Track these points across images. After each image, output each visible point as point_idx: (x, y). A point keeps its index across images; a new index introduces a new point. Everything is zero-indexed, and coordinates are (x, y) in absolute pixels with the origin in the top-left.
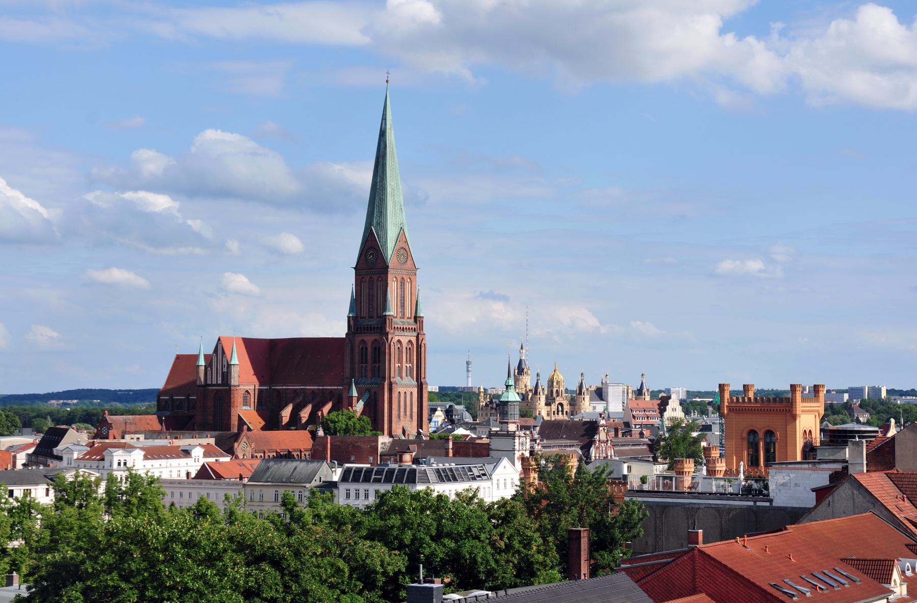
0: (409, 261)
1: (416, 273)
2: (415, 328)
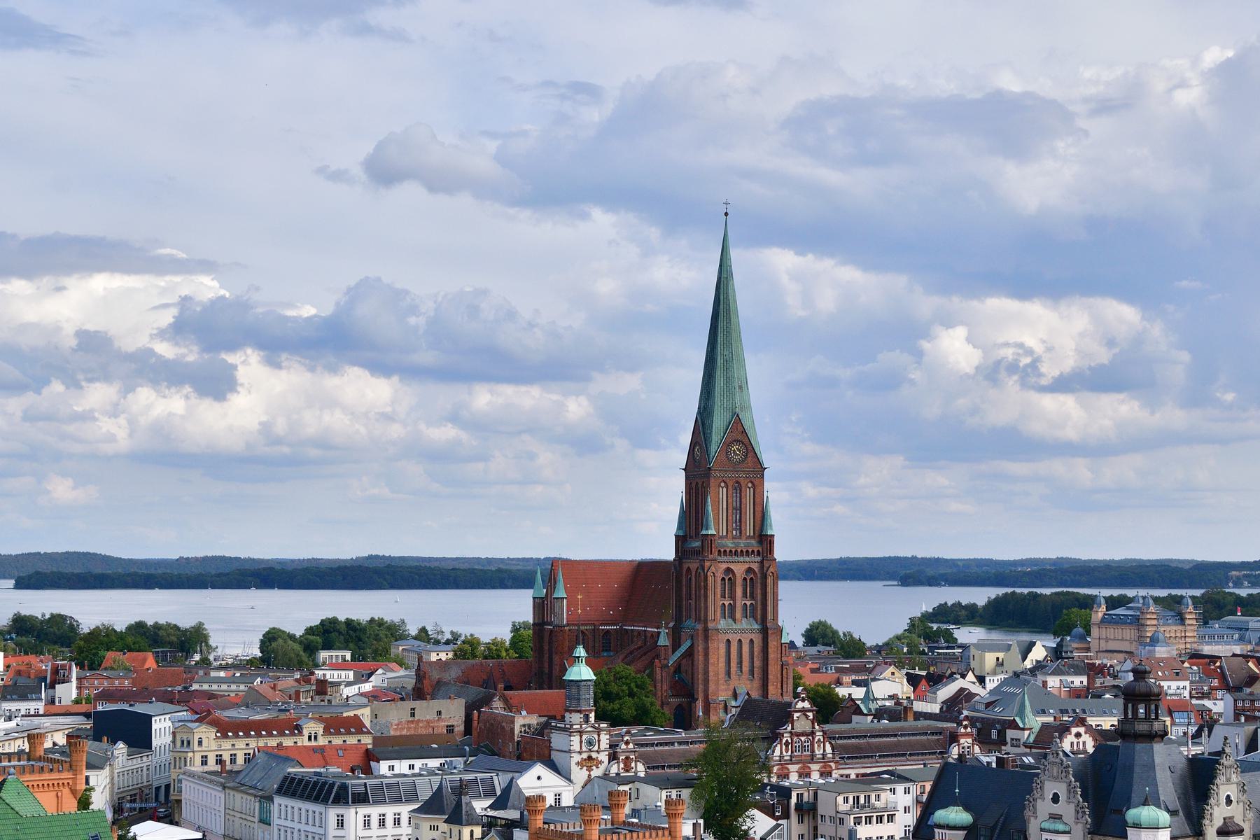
0: (749, 459)
1: (763, 475)
2: (758, 551)
